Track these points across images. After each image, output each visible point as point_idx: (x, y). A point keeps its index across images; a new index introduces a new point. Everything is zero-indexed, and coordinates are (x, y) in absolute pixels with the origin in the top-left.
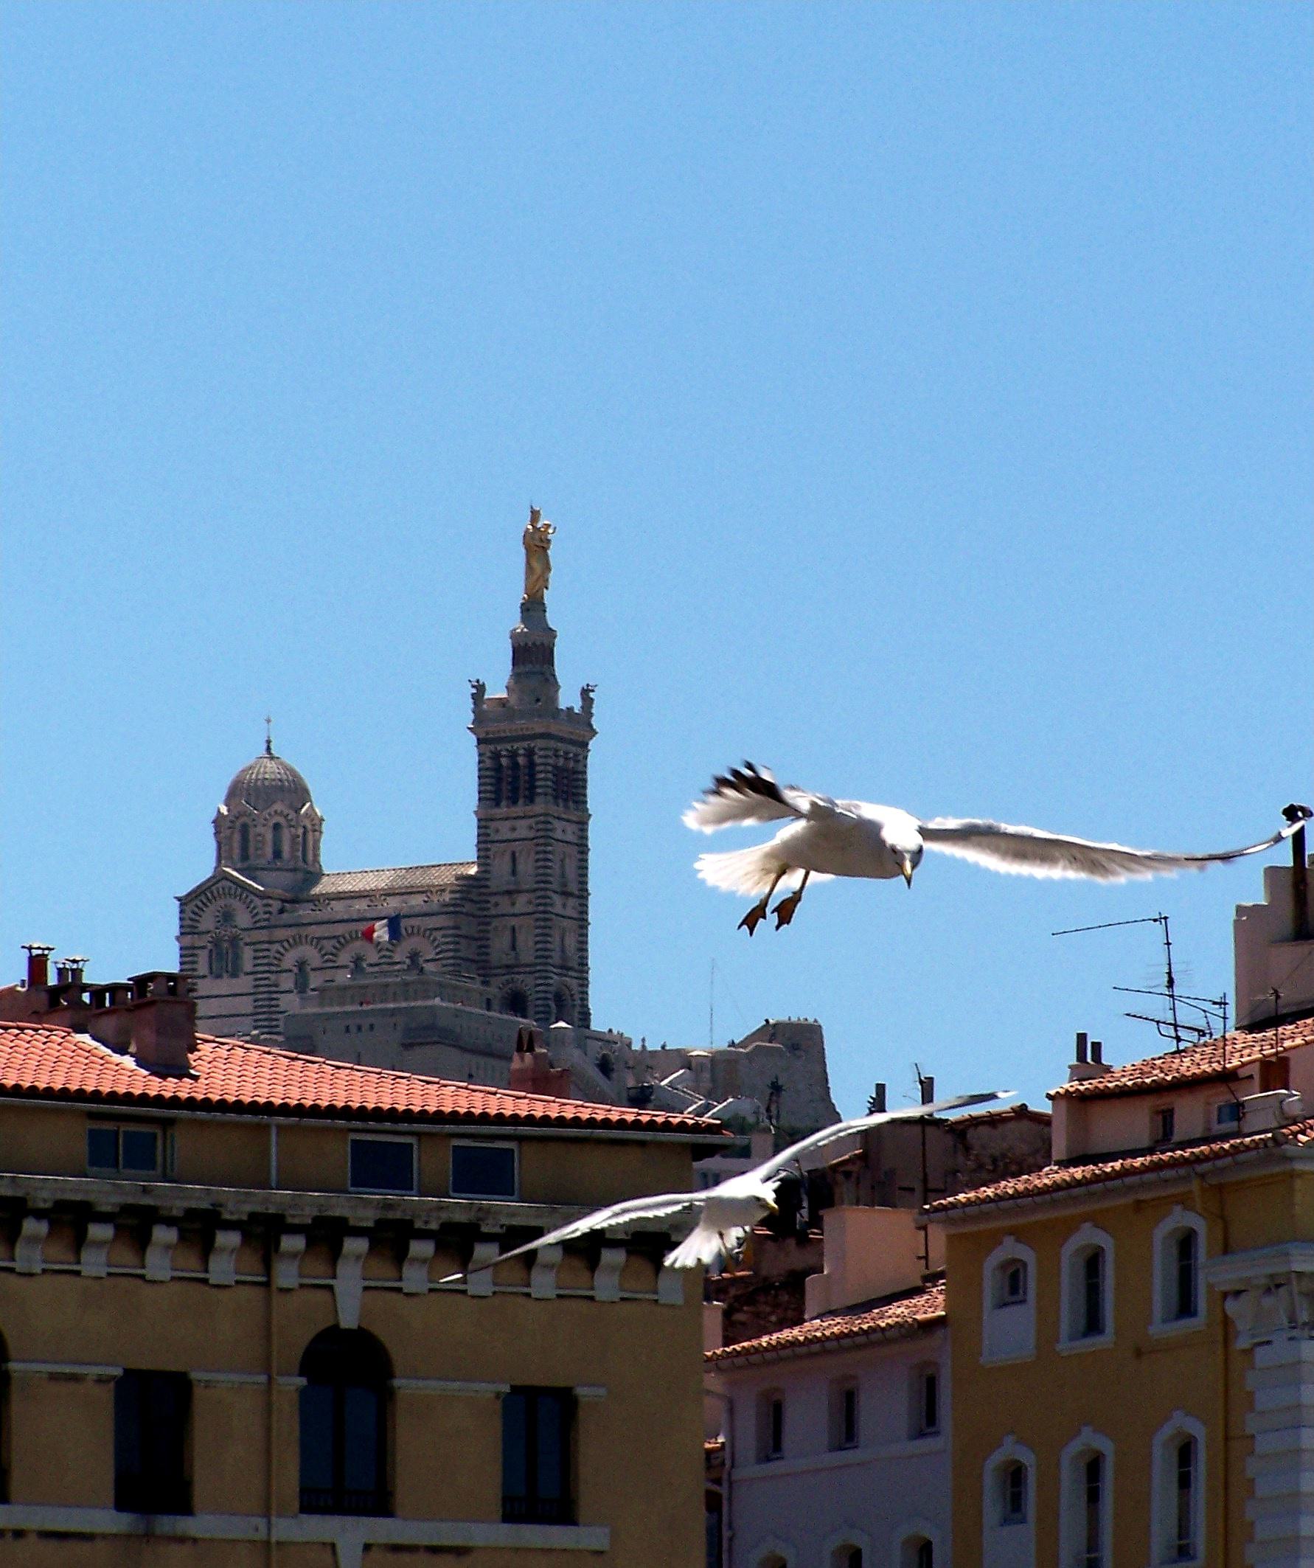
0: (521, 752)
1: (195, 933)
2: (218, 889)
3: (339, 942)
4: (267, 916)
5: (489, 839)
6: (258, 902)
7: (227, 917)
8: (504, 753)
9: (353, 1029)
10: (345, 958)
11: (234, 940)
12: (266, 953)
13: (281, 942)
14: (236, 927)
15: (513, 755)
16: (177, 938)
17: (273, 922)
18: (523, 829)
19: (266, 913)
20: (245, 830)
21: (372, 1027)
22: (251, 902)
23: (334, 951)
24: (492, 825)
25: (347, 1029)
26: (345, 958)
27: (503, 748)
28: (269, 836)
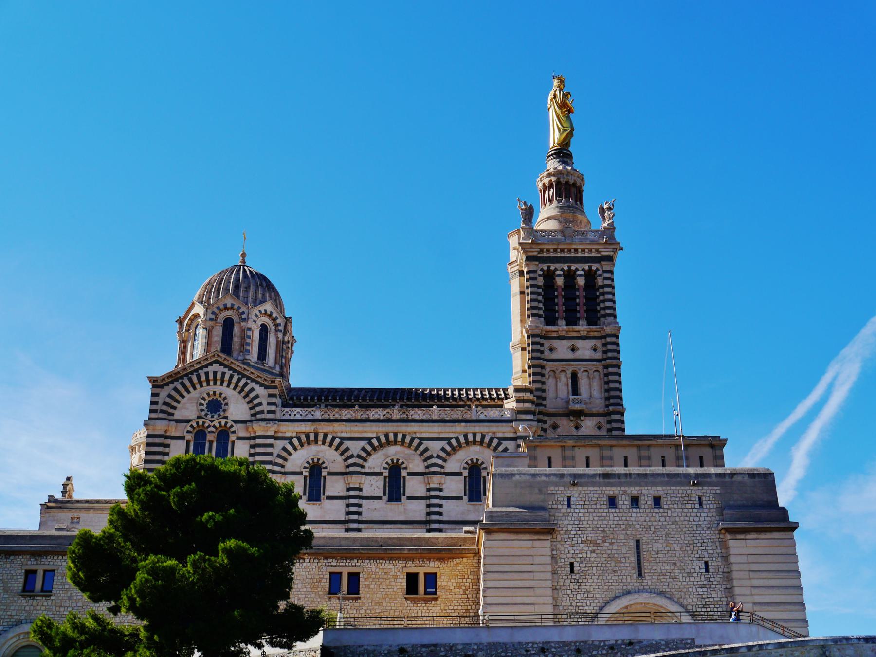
0: (580, 273)
1: (170, 420)
2: (207, 374)
3: (371, 444)
4: (273, 408)
5: (542, 356)
6: (260, 390)
7: (216, 406)
8: (558, 273)
9: (624, 502)
10: (377, 461)
11: (223, 435)
12: (269, 450)
13: (290, 439)
14: (226, 417)
15: (570, 276)
16: (146, 424)
17: (279, 416)
18: (585, 349)
19: (269, 404)
20: (228, 324)
21: (657, 501)
22: (252, 390)
23: (364, 455)
24: (547, 343)
25: (612, 502)
26: (377, 461)
27: (559, 269)
28: (256, 334)
